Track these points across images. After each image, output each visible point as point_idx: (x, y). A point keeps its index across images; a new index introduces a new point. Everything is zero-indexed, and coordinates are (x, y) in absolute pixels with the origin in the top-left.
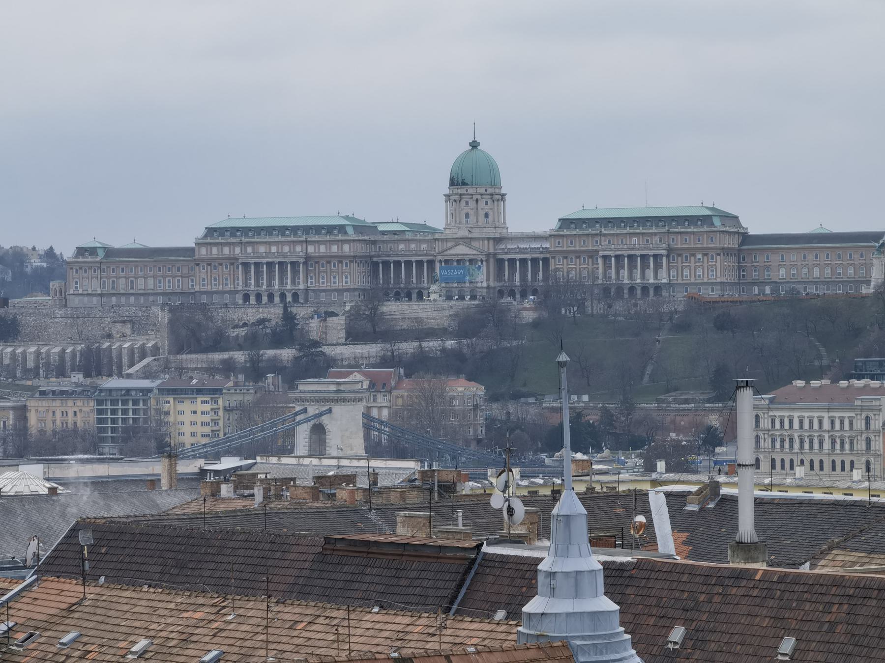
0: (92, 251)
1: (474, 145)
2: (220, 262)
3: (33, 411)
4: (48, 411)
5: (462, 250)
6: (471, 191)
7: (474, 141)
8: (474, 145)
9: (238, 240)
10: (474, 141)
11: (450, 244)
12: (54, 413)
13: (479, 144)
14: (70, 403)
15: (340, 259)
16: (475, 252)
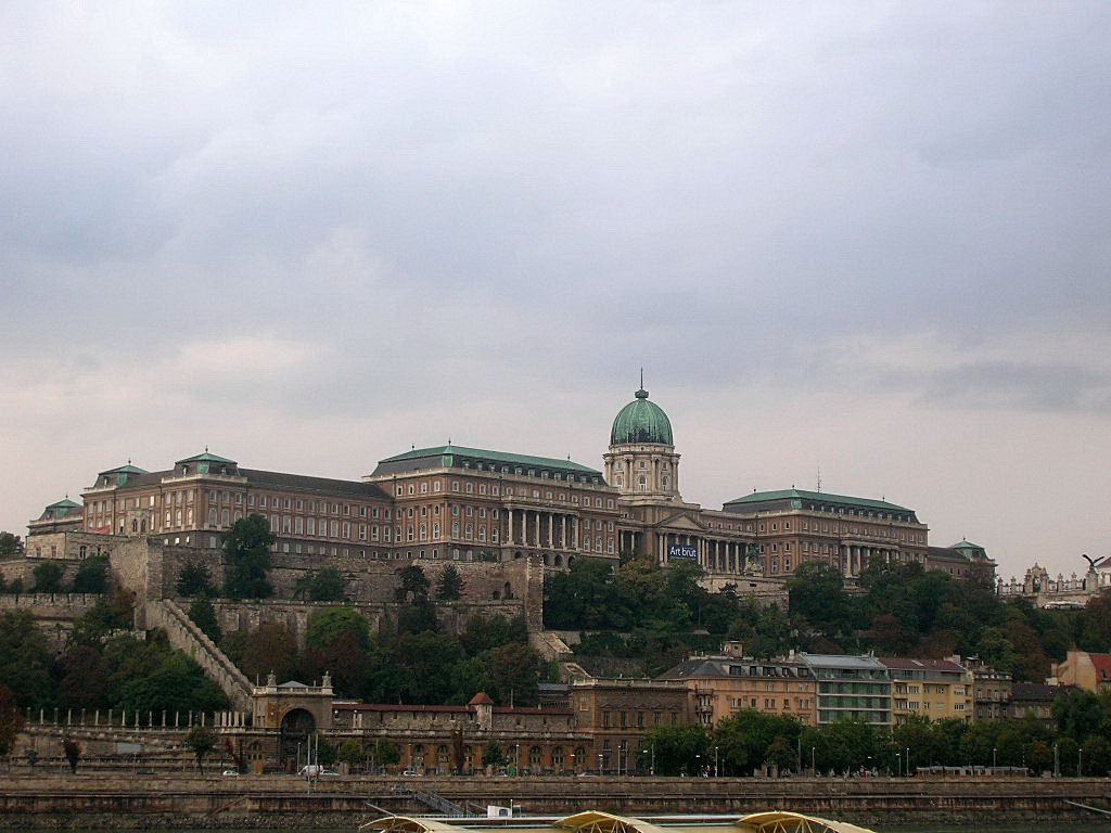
0: (228, 467)
1: (642, 395)
2: (477, 503)
3: (722, 698)
4: (745, 698)
5: (683, 523)
6: (668, 451)
7: (642, 391)
8: (642, 395)
9: (496, 476)
10: (642, 391)
11: (666, 515)
12: (753, 701)
13: (646, 395)
14: (780, 687)
15: (606, 517)
16: (696, 527)
